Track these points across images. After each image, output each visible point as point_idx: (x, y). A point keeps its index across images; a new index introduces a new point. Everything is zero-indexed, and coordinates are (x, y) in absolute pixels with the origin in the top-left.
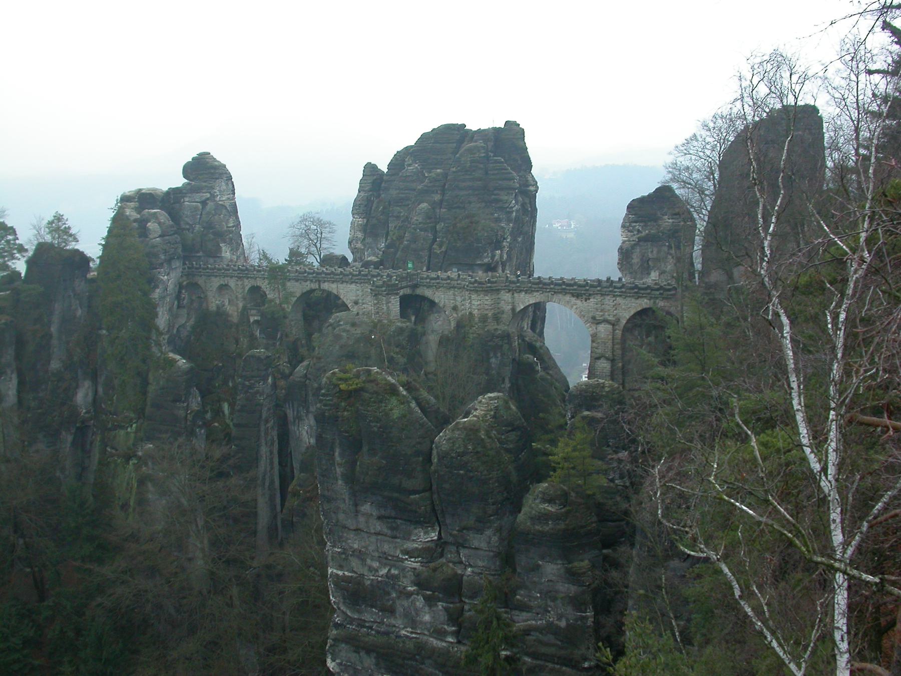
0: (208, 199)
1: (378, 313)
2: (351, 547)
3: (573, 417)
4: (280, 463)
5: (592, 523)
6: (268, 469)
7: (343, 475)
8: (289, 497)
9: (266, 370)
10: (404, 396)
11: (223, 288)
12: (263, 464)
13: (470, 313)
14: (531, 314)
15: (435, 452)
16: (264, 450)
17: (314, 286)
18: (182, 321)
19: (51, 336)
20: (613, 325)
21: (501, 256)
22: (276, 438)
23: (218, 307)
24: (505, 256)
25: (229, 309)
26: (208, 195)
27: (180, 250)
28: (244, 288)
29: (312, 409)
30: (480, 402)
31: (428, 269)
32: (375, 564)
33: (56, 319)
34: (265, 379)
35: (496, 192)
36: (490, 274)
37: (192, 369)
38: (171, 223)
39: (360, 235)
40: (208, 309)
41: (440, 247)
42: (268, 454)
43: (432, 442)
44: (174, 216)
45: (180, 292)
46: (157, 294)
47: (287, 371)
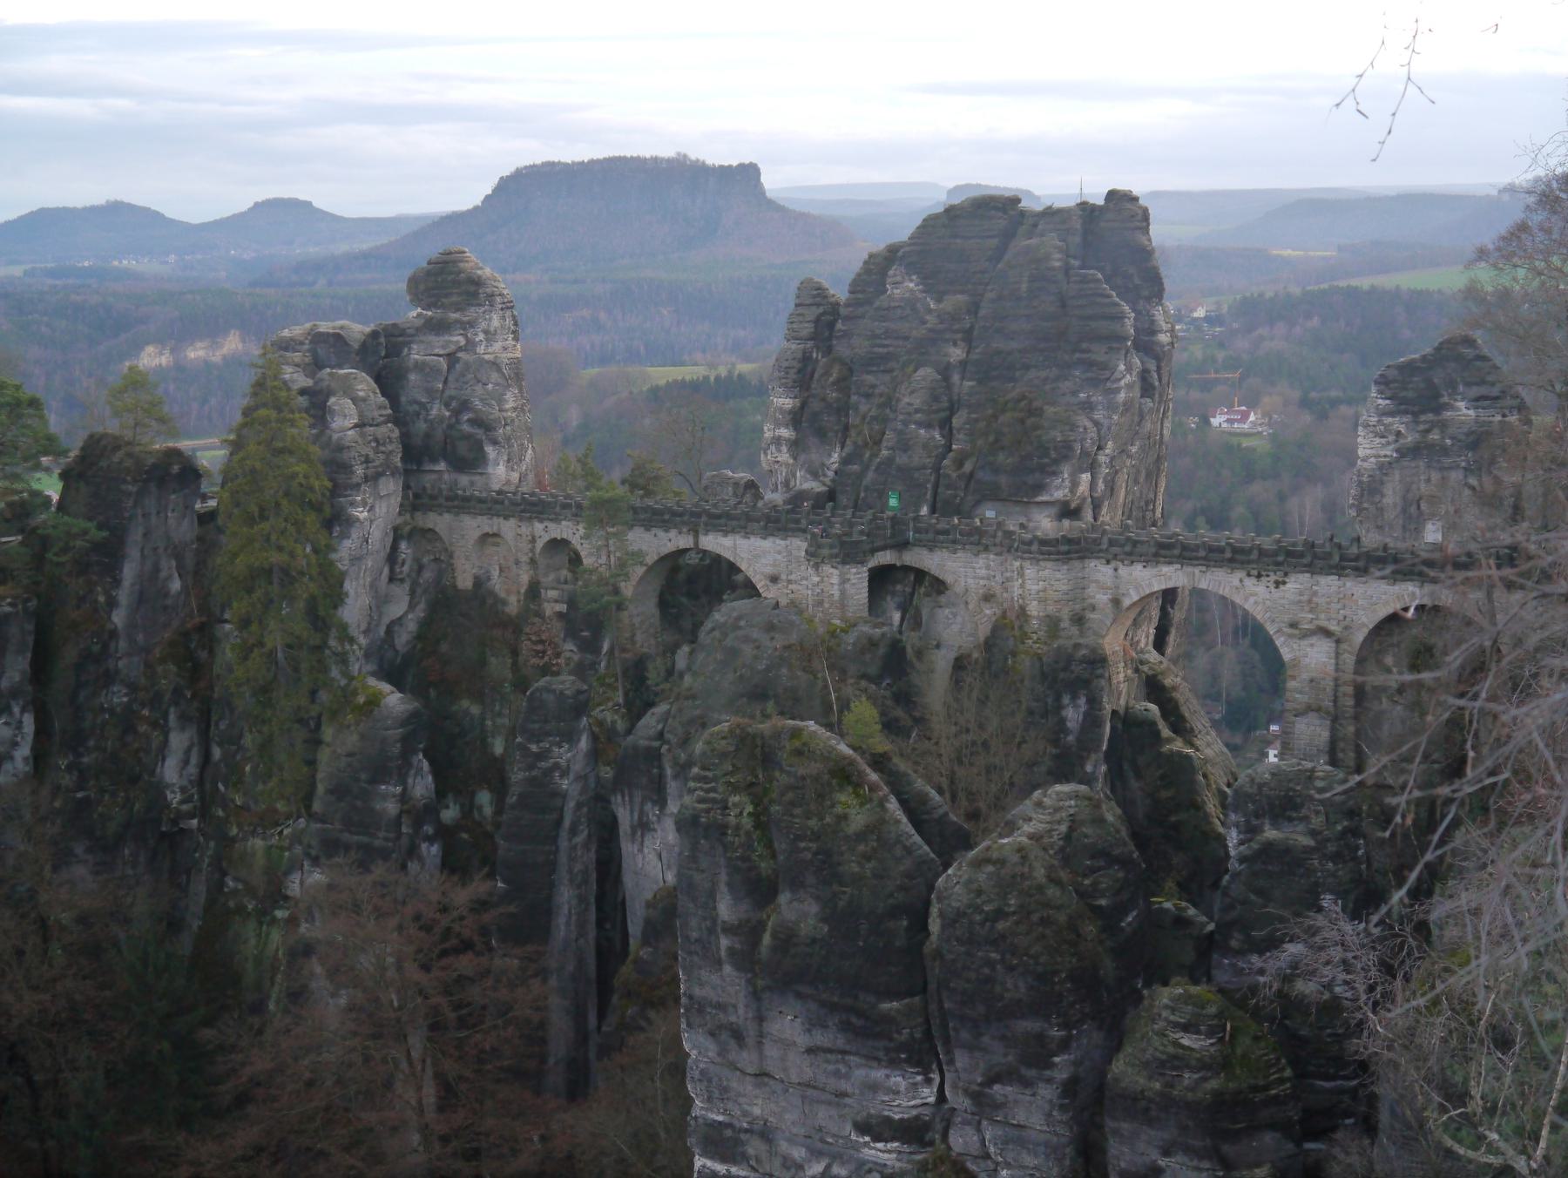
0: (460, 349)
1: (820, 603)
2: (745, 1114)
3: (1241, 843)
4: (600, 923)
5: (1281, 1081)
6: (573, 936)
7: (732, 952)
8: (615, 999)
9: (578, 716)
10: (873, 788)
11: (486, 538)
12: (562, 926)
13: (1023, 609)
14: (1155, 614)
15: (934, 910)
16: (565, 896)
17: (684, 541)
18: (397, 609)
19: (114, 634)
20: (1338, 642)
22: (592, 866)
23: (478, 582)
24: (1101, 486)
25: (497, 583)
26: (463, 342)
27: (397, 460)
28: (533, 540)
29: (673, 807)
30: (1039, 804)
31: (933, 510)
32: (798, 1153)
33: (124, 595)
34: (570, 737)
35: (1084, 345)
36: (1066, 523)
37: (414, 715)
39: (785, 433)
40: (454, 586)
41: (959, 463)
42: (574, 902)
43: (931, 887)
44: (388, 381)
45: (394, 548)
46: (346, 548)
47: (621, 726)
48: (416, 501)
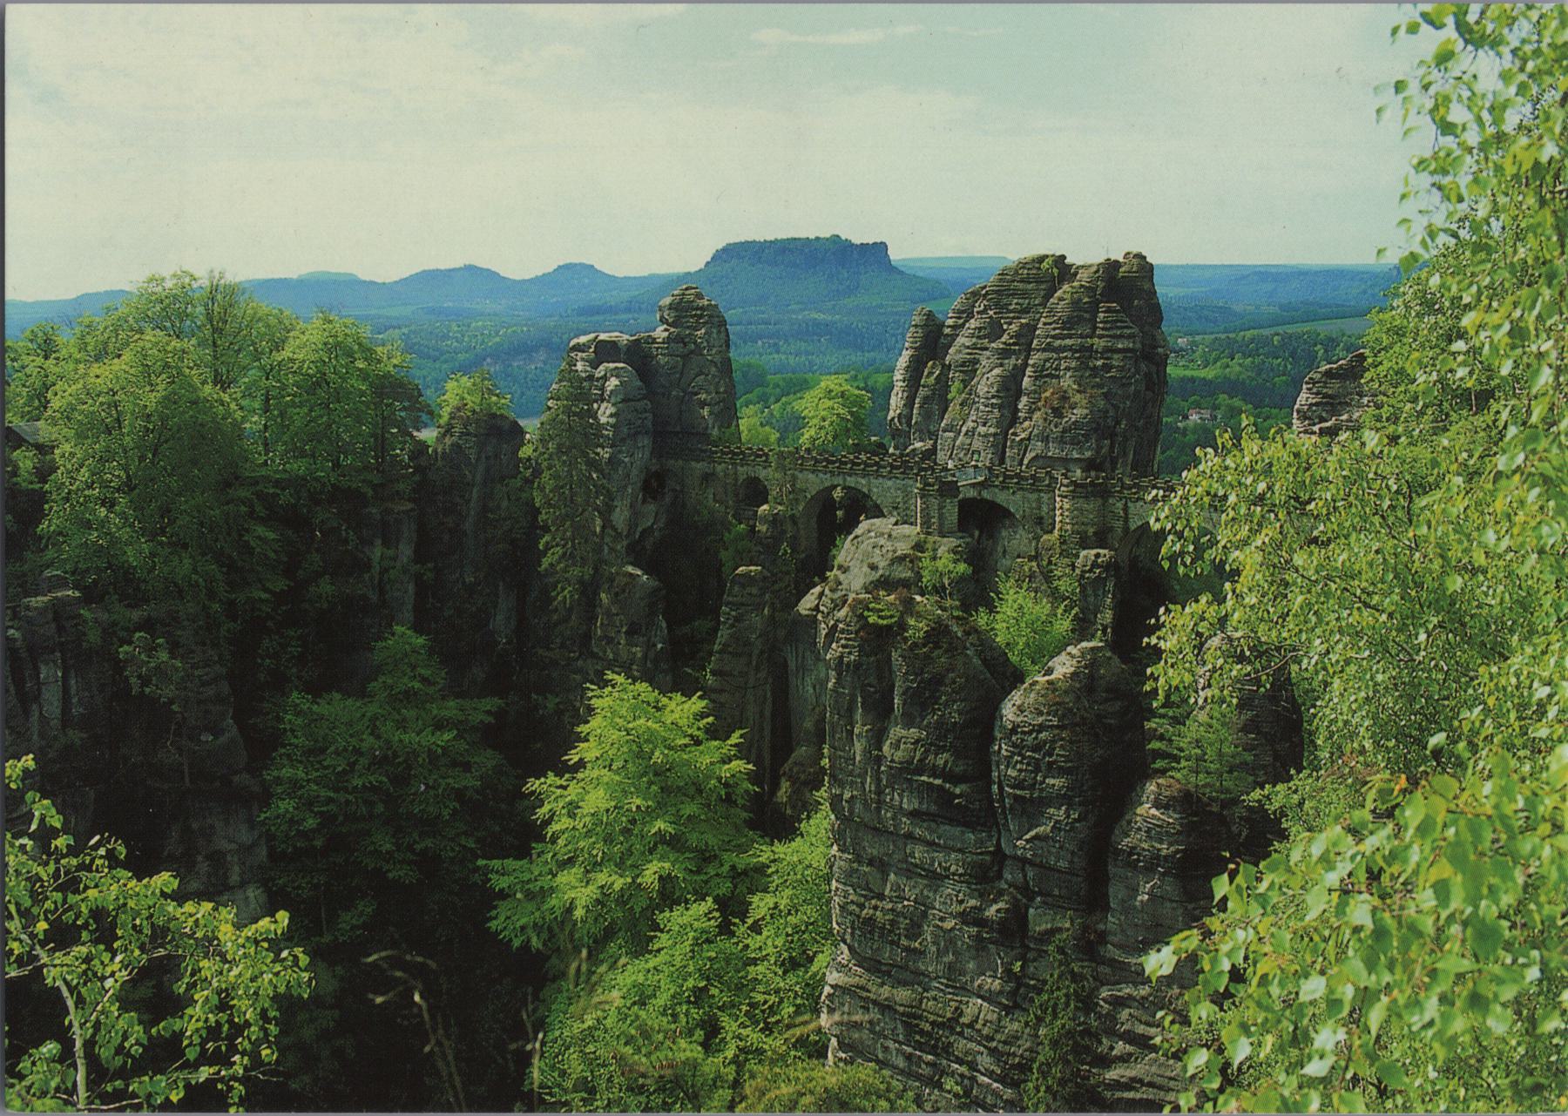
21: (1112, 446)
36: (1093, 474)
38: (639, 383)
48: (658, 451)
